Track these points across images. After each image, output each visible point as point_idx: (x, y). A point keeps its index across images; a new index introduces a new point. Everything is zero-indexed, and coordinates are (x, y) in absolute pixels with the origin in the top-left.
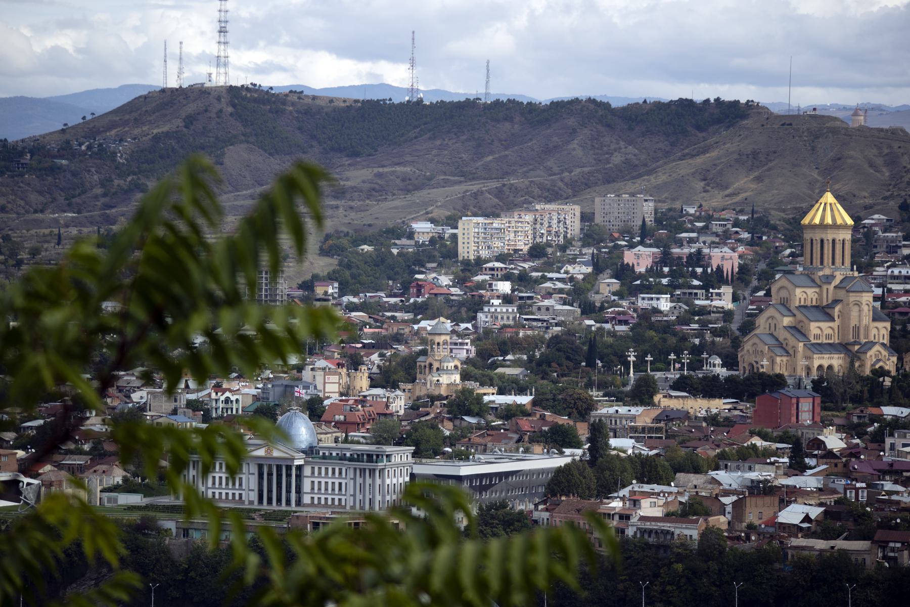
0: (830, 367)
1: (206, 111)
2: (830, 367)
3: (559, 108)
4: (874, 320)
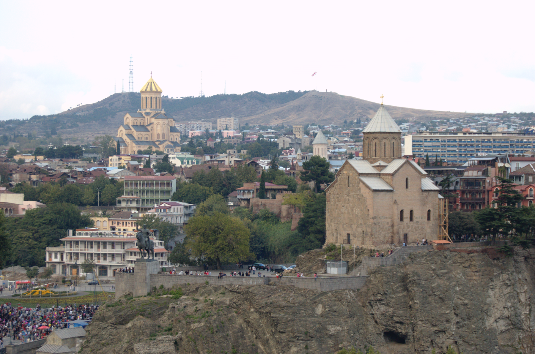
1: (118, 101)
3: (245, 95)
4: (171, 131)
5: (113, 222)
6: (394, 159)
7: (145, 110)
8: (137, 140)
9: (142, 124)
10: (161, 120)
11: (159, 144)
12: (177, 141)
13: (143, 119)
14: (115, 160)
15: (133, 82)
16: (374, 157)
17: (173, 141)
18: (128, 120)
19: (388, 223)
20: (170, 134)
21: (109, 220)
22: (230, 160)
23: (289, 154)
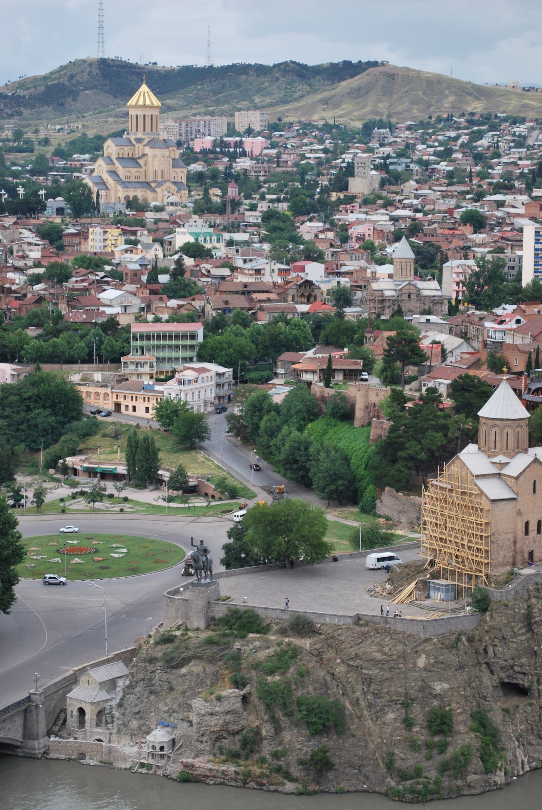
0: (135, 197)
2: (135, 197)
3: (277, 66)
4: (173, 167)
5: (117, 395)
6: (518, 453)
7: (135, 134)
8: (124, 180)
9: (130, 156)
10: (159, 150)
11: (158, 186)
12: (183, 181)
13: (133, 148)
14: (98, 234)
15: (103, 42)
16: (493, 450)
17: (176, 181)
18: (110, 150)
19: (509, 540)
20: (172, 170)
21: (112, 392)
22: (272, 268)
23: (349, 211)
